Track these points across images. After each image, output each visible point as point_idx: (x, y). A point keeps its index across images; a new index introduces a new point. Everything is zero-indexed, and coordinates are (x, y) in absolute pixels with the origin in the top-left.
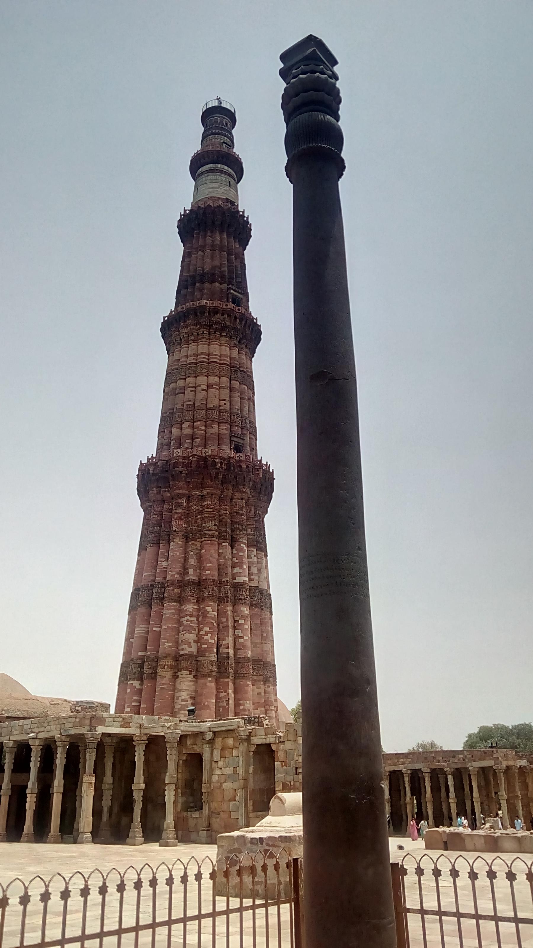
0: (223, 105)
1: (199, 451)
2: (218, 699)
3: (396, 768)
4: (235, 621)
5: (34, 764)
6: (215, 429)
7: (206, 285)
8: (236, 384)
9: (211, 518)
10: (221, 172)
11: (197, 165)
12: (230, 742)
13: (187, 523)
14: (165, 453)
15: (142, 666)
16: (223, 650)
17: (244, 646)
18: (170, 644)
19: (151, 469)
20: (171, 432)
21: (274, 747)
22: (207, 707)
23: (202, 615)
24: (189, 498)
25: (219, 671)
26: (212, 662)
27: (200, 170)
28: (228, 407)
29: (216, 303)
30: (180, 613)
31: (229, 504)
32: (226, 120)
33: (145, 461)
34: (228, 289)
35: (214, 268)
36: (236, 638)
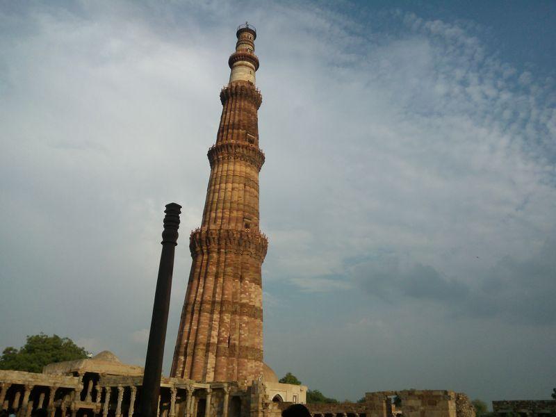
0: (250, 27)
1: (225, 227)
2: (228, 369)
3: (329, 413)
4: (241, 325)
5: (120, 399)
6: (235, 214)
7: (236, 131)
8: (248, 188)
9: (229, 265)
10: (246, 66)
11: (233, 62)
12: (220, 394)
13: (217, 267)
14: (207, 226)
15: (186, 348)
16: (232, 342)
17: (245, 340)
18: (202, 336)
19: (198, 235)
20: (210, 215)
21: (241, 398)
22: (221, 374)
23: (221, 321)
24: (219, 253)
25: (230, 353)
26: (225, 348)
27: (235, 64)
28: (242, 202)
29: (239, 142)
30: (211, 320)
31: (241, 257)
32: (251, 36)
33: (194, 231)
34: (246, 133)
35: (239, 121)
36: (240, 334)
